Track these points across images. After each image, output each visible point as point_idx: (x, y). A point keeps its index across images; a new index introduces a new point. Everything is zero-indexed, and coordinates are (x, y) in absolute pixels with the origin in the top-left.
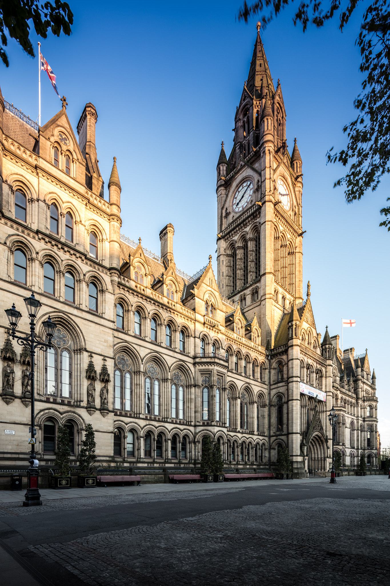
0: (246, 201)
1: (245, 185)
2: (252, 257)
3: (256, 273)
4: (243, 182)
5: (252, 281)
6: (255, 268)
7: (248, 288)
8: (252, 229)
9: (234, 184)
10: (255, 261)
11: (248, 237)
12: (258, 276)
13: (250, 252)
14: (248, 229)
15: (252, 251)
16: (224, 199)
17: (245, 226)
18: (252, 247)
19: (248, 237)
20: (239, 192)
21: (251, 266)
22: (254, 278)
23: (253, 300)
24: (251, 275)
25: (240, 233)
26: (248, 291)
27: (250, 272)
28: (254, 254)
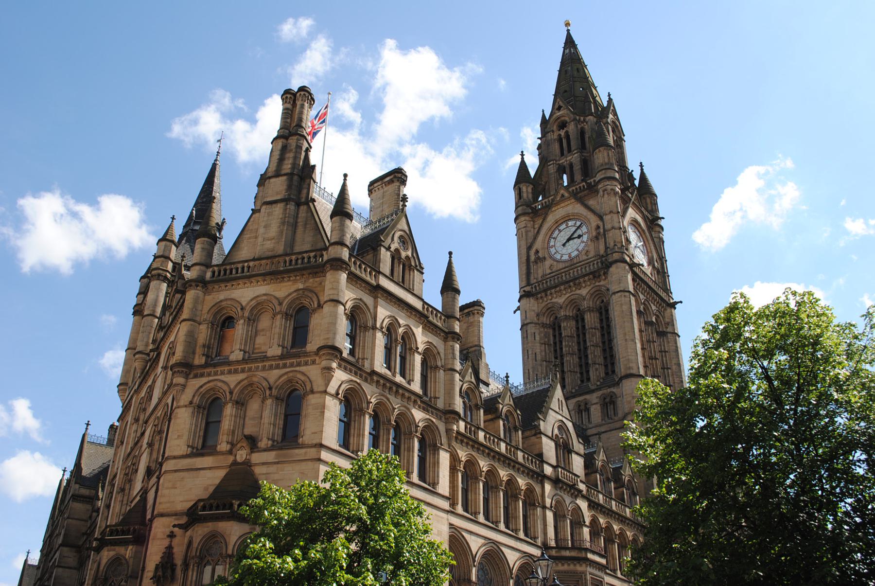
0: (575, 247)
1: (570, 223)
2: (594, 338)
3: (606, 366)
4: (567, 219)
5: (598, 381)
6: (602, 357)
7: (593, 391)
8: (592, 295)
9: (551, 219)
10: (601, 345)
11: (585, 304)
12: (610, 373)
13: (591, 330)
14: (584, 292)
15: (595, 329)
16: (531, 234)
17: (579, 286)
18: (595, 322)
19: (585, 304)
20: (560, 231)
21: (595, 354)
22: (603, 375)
23: (605, 414)
24: (596, 370)
25: (568, 295)
26: (594, 398)
27: (595, 364)
28: (598, 334)
